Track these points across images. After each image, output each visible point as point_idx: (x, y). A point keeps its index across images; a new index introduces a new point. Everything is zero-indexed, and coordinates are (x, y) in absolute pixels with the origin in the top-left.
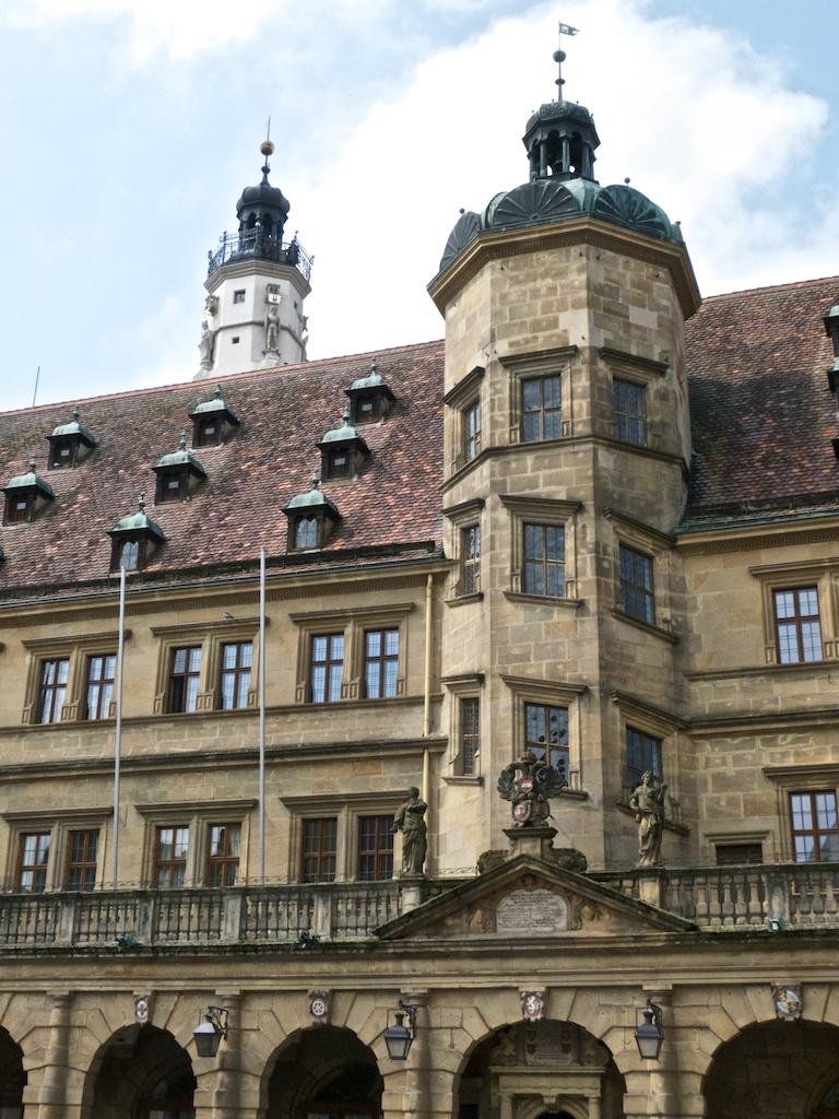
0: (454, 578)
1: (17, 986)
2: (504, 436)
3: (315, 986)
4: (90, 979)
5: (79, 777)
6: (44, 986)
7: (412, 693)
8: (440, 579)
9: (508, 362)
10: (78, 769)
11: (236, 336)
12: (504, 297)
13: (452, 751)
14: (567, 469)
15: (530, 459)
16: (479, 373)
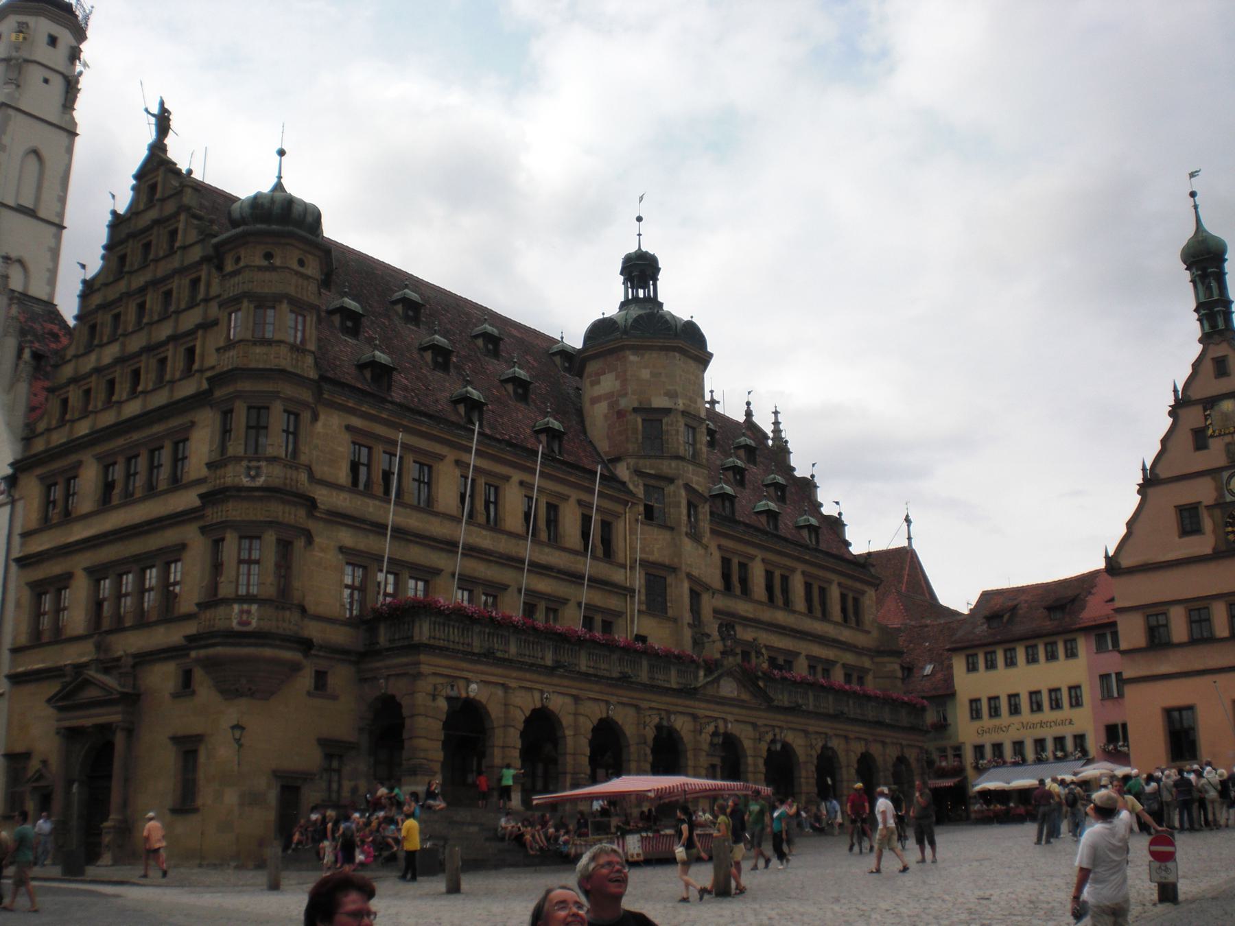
1: (558, 689)
2: (682, 453)
3: (672, 708)
5: (491, 561)
6: (574, 692)
7: (621, 560)
8: (633, 504)
9: (685, 413)
10: (495, 557)
11: (47, 77)
14: (701, 479)
15: (691, 468)
16: (667, 411)
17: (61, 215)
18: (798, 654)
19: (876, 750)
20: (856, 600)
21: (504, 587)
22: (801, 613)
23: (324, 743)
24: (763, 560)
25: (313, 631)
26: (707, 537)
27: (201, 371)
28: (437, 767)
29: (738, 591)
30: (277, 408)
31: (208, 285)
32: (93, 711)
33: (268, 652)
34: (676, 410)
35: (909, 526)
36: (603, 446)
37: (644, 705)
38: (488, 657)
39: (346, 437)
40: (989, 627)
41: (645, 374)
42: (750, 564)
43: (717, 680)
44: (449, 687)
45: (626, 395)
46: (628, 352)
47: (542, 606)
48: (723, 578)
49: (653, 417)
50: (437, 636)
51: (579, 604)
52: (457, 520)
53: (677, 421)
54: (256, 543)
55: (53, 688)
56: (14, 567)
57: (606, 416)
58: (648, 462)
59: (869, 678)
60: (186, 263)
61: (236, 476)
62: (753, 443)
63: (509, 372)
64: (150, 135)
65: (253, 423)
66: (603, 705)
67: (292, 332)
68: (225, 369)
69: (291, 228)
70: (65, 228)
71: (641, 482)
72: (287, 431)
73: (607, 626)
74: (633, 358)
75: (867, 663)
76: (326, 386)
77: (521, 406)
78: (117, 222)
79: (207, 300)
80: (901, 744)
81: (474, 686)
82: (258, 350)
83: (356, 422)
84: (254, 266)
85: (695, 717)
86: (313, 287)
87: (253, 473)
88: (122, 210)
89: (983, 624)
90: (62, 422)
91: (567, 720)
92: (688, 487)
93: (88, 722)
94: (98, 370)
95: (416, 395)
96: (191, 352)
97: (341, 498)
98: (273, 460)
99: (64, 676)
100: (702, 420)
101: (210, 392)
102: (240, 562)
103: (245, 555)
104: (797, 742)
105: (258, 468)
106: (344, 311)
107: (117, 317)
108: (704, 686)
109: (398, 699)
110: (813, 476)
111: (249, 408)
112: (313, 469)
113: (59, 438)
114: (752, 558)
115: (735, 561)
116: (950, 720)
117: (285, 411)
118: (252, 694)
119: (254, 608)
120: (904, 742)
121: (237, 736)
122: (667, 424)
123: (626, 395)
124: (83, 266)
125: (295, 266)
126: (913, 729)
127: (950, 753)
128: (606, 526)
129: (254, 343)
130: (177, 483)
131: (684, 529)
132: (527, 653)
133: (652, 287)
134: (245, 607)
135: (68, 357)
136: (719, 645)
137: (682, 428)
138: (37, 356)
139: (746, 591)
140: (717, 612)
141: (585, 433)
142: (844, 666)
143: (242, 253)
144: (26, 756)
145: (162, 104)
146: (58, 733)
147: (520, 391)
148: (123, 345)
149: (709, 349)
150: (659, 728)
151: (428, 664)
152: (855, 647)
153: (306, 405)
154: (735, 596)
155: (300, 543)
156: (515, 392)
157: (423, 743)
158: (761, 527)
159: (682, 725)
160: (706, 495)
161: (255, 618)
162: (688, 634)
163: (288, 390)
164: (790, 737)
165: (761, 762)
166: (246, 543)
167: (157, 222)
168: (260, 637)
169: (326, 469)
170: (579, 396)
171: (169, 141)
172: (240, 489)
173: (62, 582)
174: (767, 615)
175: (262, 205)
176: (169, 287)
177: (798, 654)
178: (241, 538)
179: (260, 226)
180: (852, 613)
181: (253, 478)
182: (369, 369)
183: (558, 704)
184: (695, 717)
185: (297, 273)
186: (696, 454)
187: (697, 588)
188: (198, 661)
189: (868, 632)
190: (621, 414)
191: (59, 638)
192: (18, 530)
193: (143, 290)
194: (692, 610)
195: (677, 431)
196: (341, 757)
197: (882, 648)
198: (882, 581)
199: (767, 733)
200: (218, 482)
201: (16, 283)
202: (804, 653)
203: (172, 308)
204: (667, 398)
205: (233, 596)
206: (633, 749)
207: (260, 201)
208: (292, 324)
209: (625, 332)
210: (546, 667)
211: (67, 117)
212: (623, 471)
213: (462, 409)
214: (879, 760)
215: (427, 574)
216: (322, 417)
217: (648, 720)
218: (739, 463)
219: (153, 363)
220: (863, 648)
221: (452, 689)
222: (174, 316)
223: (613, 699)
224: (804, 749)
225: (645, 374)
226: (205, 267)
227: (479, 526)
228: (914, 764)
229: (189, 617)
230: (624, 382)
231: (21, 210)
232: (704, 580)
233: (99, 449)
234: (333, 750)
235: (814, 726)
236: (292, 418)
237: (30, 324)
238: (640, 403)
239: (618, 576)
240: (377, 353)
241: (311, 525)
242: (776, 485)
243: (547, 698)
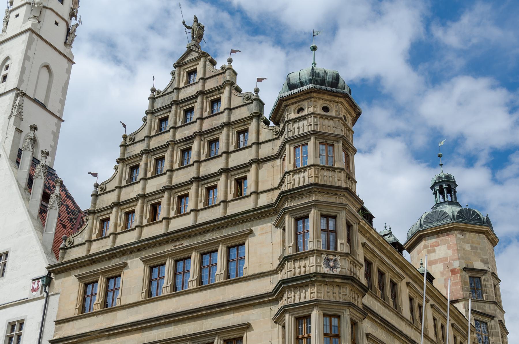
16: (485, 272)
17: (61, 111)
31: (258, 133)
57: (442, 273)
60: (232, 120)
68: (296, 186)
82: (326, 173)
84: (318, 114)
87: (332, 264)
90: (101, 236)
105: (335, 260)
122: (485, 280)
124: (124, 126)
145: (196, 19)
148: (171, 177)
172: (324, 276)
176: (216, 137)
181: (332, 268)
190: (453, 272)
193: (190, 139)
200: (297, 271)
204: (483, 263)
231: (35, 101)
233: (145, 254)
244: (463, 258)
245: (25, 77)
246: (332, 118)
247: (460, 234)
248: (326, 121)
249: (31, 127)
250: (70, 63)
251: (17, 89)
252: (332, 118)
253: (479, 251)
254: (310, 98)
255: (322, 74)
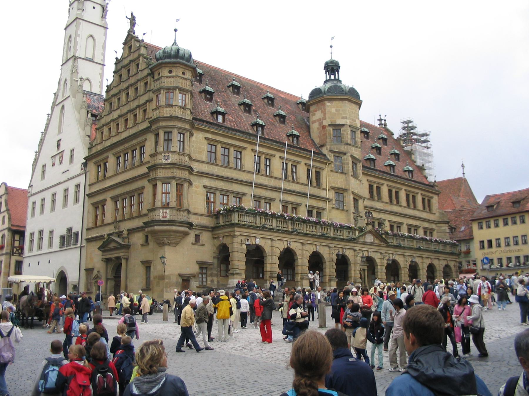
0: (333, 166)
2: (349, 142)
3: (343, 247)
4: (310, 240)
6: (302, 241)
7: (325, 187)
8: (329, 164)
9: (350, 126)
11: (94, 6)
12: (348, 111)
13: (334, 202)
15: (353, 148)
16: (343, 125)
17: (103, 60)
18: (402, 224)
19: (435, 262)
20: (429, 201)
21: (273, 200)
22: (404, 207)
23: (198, 262)
24: (387, 185)
25: (194, 220)
26: (361, 176)
27: (148, 119)
28: (243, 272)
29: (376, 198)
30: (175, 131)
31: (150, 85)
32: (114, 252)
33: (174, 228)
34: (347, 124)
35: (463, 168)
36: (317, 141)
37: (331, 246)
38: (263, 228)
39: (206, 142)
40: (488, 210)
41: (333, 110)
42: (382, 187)
43: (365, 234)
44: (247, 240)
45: (325, 119)
46: (326, 102)
47: (290, 207)
48: (369, 192)
49: (337, 127)
50: (242, 220)
51: (306, 206)
52: (253, 173)
53: (347, 129)
54: (169, 185)
55: (100, 243)
56: (86, 197)
57: (318, 129)
58: (335, 146)
59: (435, 233)
61: (161, 160)
62: (386, 137)
63: (277, 113)
64: (128, 27)
65: (166, 138)
66: (314, 246)
67: (180, 101)
69: (179, 60)
70: (105, 65)
71: (332, 155)
72: (180, 141)
73: (319, 214)
74: (328, 104)
75: (434, 226)
76: (195, 122)
77: (282, 125)
78: (118, 62)
79: (150, 91)
80: (447, 260)
81: (258, 240)
82: (168, 109)
83: (209, 136)
85: (354, 250)
86: (189, 83)
87: (166, 158)
88: (119, 58)
89: (485, 209)
91: (298, 253)
92: (352, 156)
93: (112, 256)
94: (113, 120)
95: (236, 123)
96: (145, 111)
97: (204, 166)
98: (174, 152)
99: (104, 238)
100: (358, 129)
101: (151, 127)
102: (163, 193)
103: (164, 190)
104: (400, 259)
106: (205, 91)
107: (119, 99)
108: (358, 238)
109: (227, 245)
110: (412, 150)
111: (165, 132)
112: (191, 155)
113: (99, 148)
114: (382, 184)
115: (375, 186)
116: (471, 250)
117: (179, 133)
118: (169, 244)
119: (168, 211)
120: (448, 259)
121: (163, 261)
122: (343, 130)
123: (325, 119)
125: (181, 75)
126: (452, 254)
127: (471, 263)
128: (318, 174)
129: (166, 107)
130: (142, 163)
131: (351, 173)
132: (281, 226)
133: (337, 74)
134: (165, 211)
135: (103, 116)
136: (366, 222)
137: (349, 132)
138: (93, 115)
139: (380, 198)
140: (365, 207)
141: (310, 135)
142: (423, 228)
143: (160, 71)
144: (92, 270)
145: (132, 14)
146: (102, 261)
147: (282, 120)
149: (361, 99)
150: (338, 255)
151: (238, 231)
152: (428, 220)
153: (187, 130)
154: (375, 200)
155: (186, 185)
156: (279, 120)
157: (236, 262)
158: (387, 171)
159: (349, 254)
160: (360, 159)
161: (168, 214)
162: (352, 216)
163: (179, 124)
164: (397, 258)
165: (384, 268)
166: (164, 185)
167: (131, 61)
168: (171, 222)
169: (197, 155)
170: (309, 121)
171: (136, 29)
172: (161, 164)
173: (103, 203)
174: (389, 208)
175: (167, 51)
176: (137, 86)
177: (402, 224)
178: (163, 183)
179: (167, 60)
180: (427, 205)
182: (215, 114)
183: (295, 246)
184: (354, 250)
185: (182, 78)
186: (356, 142)
187: (357, 198)
188: (148, 232)
189: (435, 214)
190: (324, 127)
191: (103, 225)
192: (88, 183)
193: (127, 88)
194: (354, 207)
195: (347, 133)
196: (206, 268)
197: (440, 220)
198: (440, 192)
199: (386, 256)
201: (86, 87)
202: (405, 223)
203: (138, 95)
205: (160, 206)
206: (327, 263)
207: (166, 50)
208: (180, 98)
209: (325, 93)
210: (289, 231)
211: (104, 22)
212: (325, 151)
213: (255, 128)
214: (437, 267)
215: (240, 196)
216: (195, 135)
217: (333, 252)
218: (379, 145)
219: (132, 116)
220: (432, 221)
221: (248, 241)
222: (138, 98)
223: (318, 244)
224: (404, 263)
225: (333, 110)
226: (149, 77)
227: (263, 175)
228: (453, 269)
229: (146, 215)
230: (325, 114)
231: (87, 59)
232: (360, 194)
233: (114, 151)
234: (203, 266)
235: (407, 253)
236: (182, 135)
237: (92, 103)
238: (332, 123)
239: (323, 194)
240: (219, 108)
241: (192, 178)
242: (395, 154)
243: (289, 244)
244: (329, 118)
245: (78, 47)
246: (173, 77)
247: (328, 102)
248: (170, 80)
249: (80, 78)
250: (106, 29)
251: (73, 56)
252: (173, 77)
253: (341, 112)
254: (162, 67)
255: (169, 51)
